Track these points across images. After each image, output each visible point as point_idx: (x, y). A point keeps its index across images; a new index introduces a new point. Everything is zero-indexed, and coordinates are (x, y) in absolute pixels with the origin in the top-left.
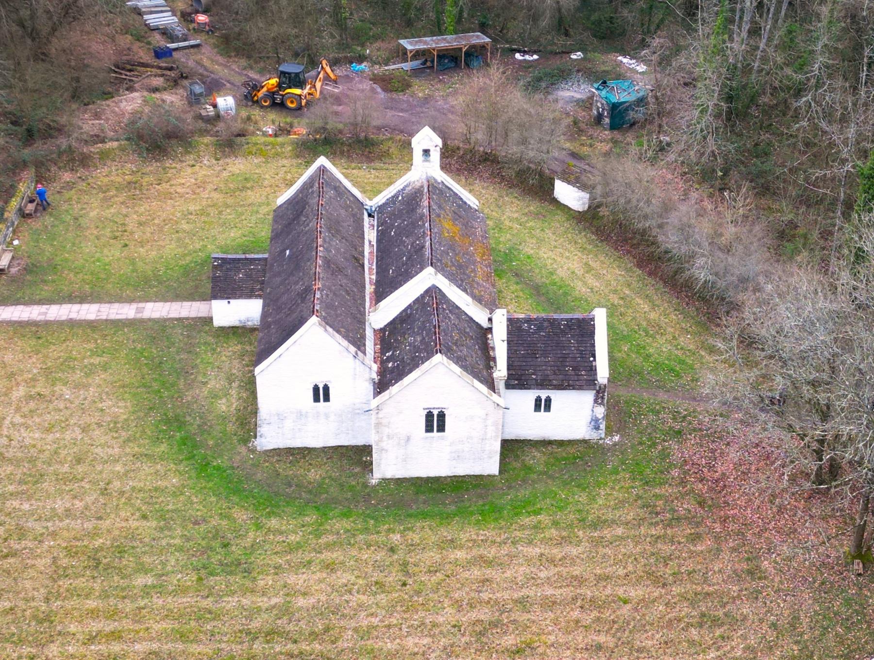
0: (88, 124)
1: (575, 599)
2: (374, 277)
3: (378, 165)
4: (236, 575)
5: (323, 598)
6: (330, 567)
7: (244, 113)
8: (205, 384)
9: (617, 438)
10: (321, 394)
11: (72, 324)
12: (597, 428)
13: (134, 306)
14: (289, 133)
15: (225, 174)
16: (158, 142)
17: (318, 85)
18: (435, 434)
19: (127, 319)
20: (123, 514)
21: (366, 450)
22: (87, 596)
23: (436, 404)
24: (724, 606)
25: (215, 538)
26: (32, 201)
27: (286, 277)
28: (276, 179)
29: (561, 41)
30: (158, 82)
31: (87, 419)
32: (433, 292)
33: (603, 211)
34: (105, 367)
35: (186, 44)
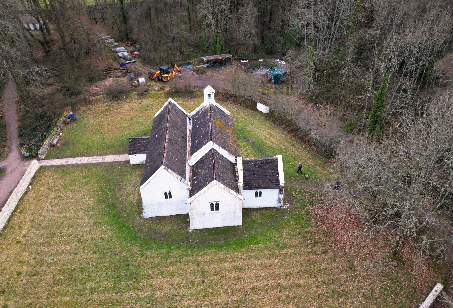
0: (93, 89)
1: (277, 286)
2: (190, 144)
3: (194, 99)
4: (131, 280)
5: (168, 292)
6: (171, 275)
7: (148, 84)
8: (125, 189)
9: (288, 205)
10: (168, 195)
11: (77, 165)
12: (280, 202)
13: (102, 157)
14: (163, 90)
15: (140, 105)
16: (117, 95)
17: (174, 73)
18: (215, 211)
19: (98, 163)
20: (86, 251)
21: (187, 216)
22: (65, 295)
23: (214, 200)
24: (341, 286)
25: (123, 262)
26: (69, 118)
28: (159, 105)
29: (256, 56)
30: (120, 74)
31: (77, 207)
32: (212, 151)
33: (276, 114)
34: (87, 184)
35: (131, 61)
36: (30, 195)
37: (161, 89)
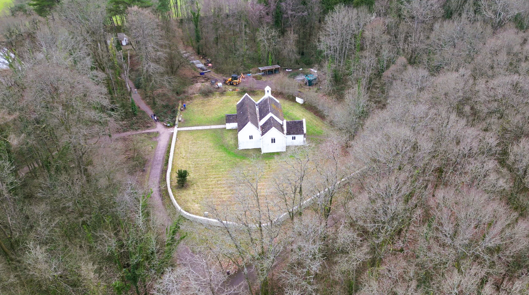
10: (251, 137)
11: (197, 130)
16: (206, 94)
21: (260, 149)
23: (273, 137)
27: (241, 117)
29: (297, 66)
30: (203, 80)
32: (271, 117)
34: (206, 137)
36: (179, 142)
37: (233, 90)
